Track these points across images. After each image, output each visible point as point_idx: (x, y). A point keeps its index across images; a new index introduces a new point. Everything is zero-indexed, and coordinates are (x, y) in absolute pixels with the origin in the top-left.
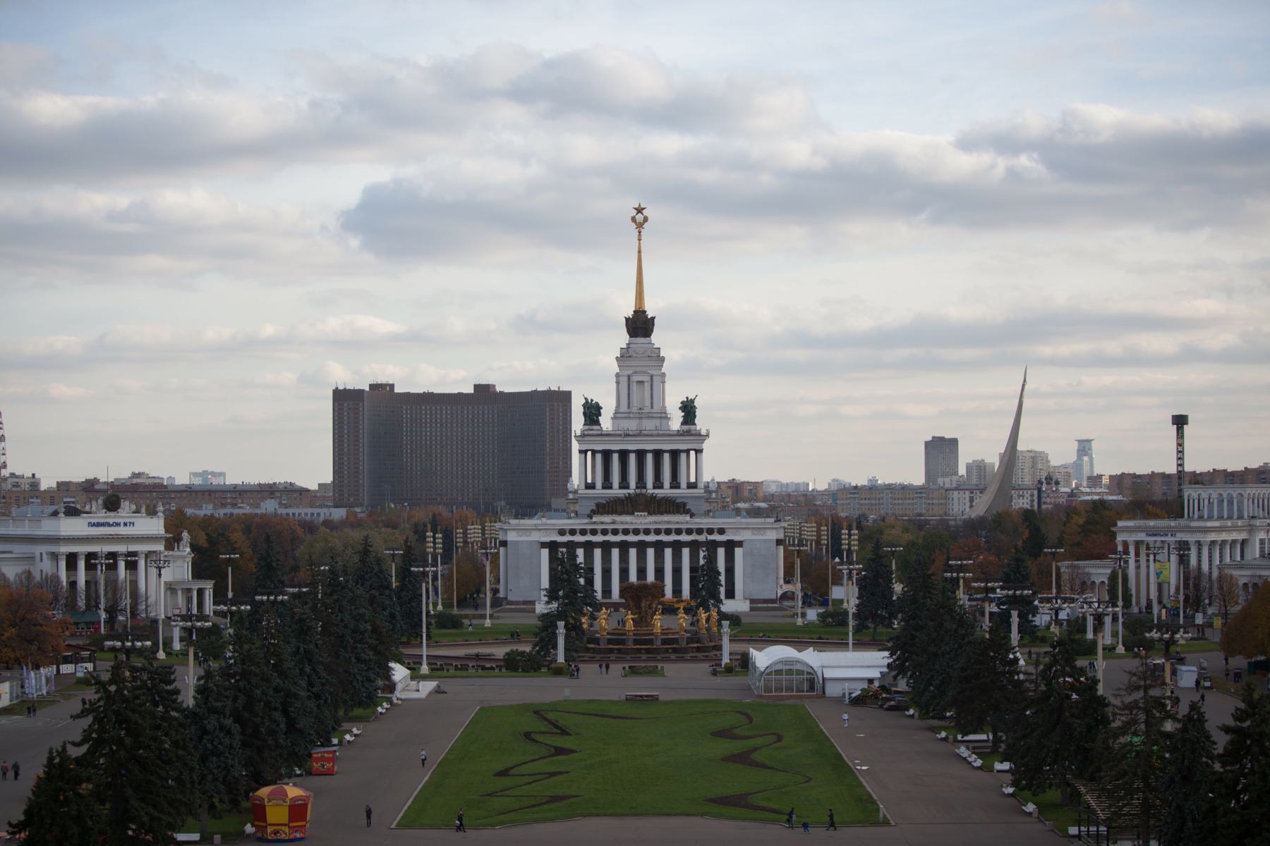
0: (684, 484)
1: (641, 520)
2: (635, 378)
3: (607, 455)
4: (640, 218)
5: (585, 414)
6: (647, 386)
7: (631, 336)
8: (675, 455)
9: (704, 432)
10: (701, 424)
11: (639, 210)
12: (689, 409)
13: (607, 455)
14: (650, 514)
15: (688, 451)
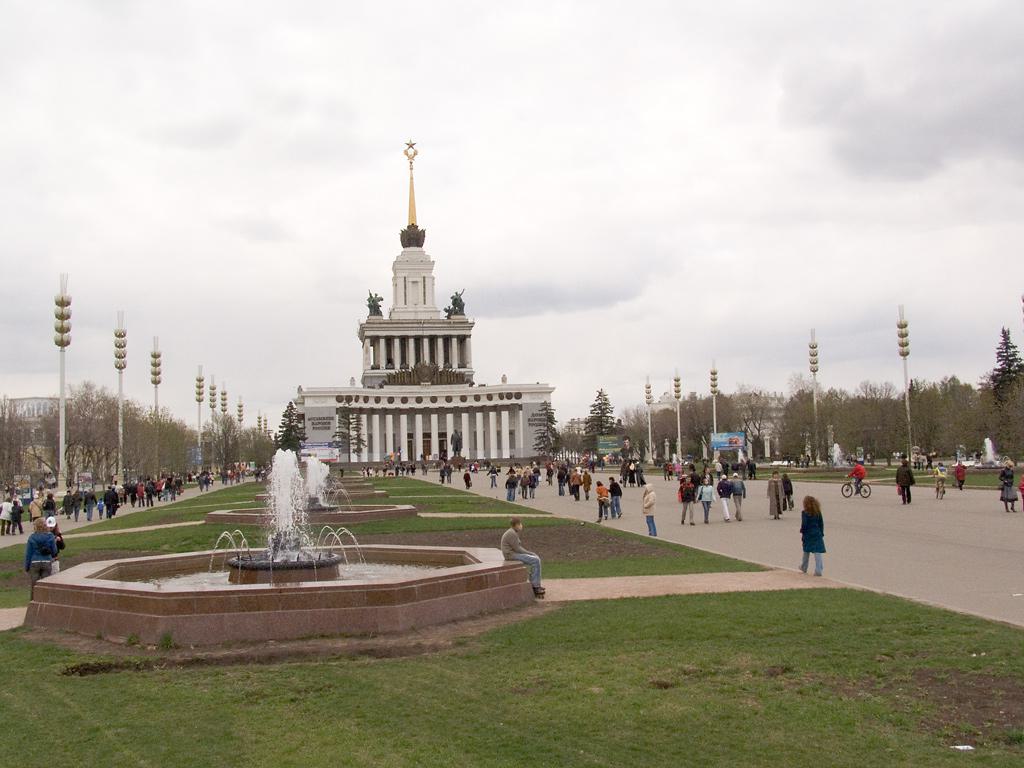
0: (455, 366)
1: (426, 390)
2: (411, 280)
3: (389, 340)
4: (411, 152)
5: (370, 306)
6: (421, 285)
7: (404, 246)
8: (447, 339)
9: (470, 321)
10: (469, 314)
11: (411, 146)
12: (458, 305)
13: (389, 340)
14: (433, 384)
15: (458, 337)
